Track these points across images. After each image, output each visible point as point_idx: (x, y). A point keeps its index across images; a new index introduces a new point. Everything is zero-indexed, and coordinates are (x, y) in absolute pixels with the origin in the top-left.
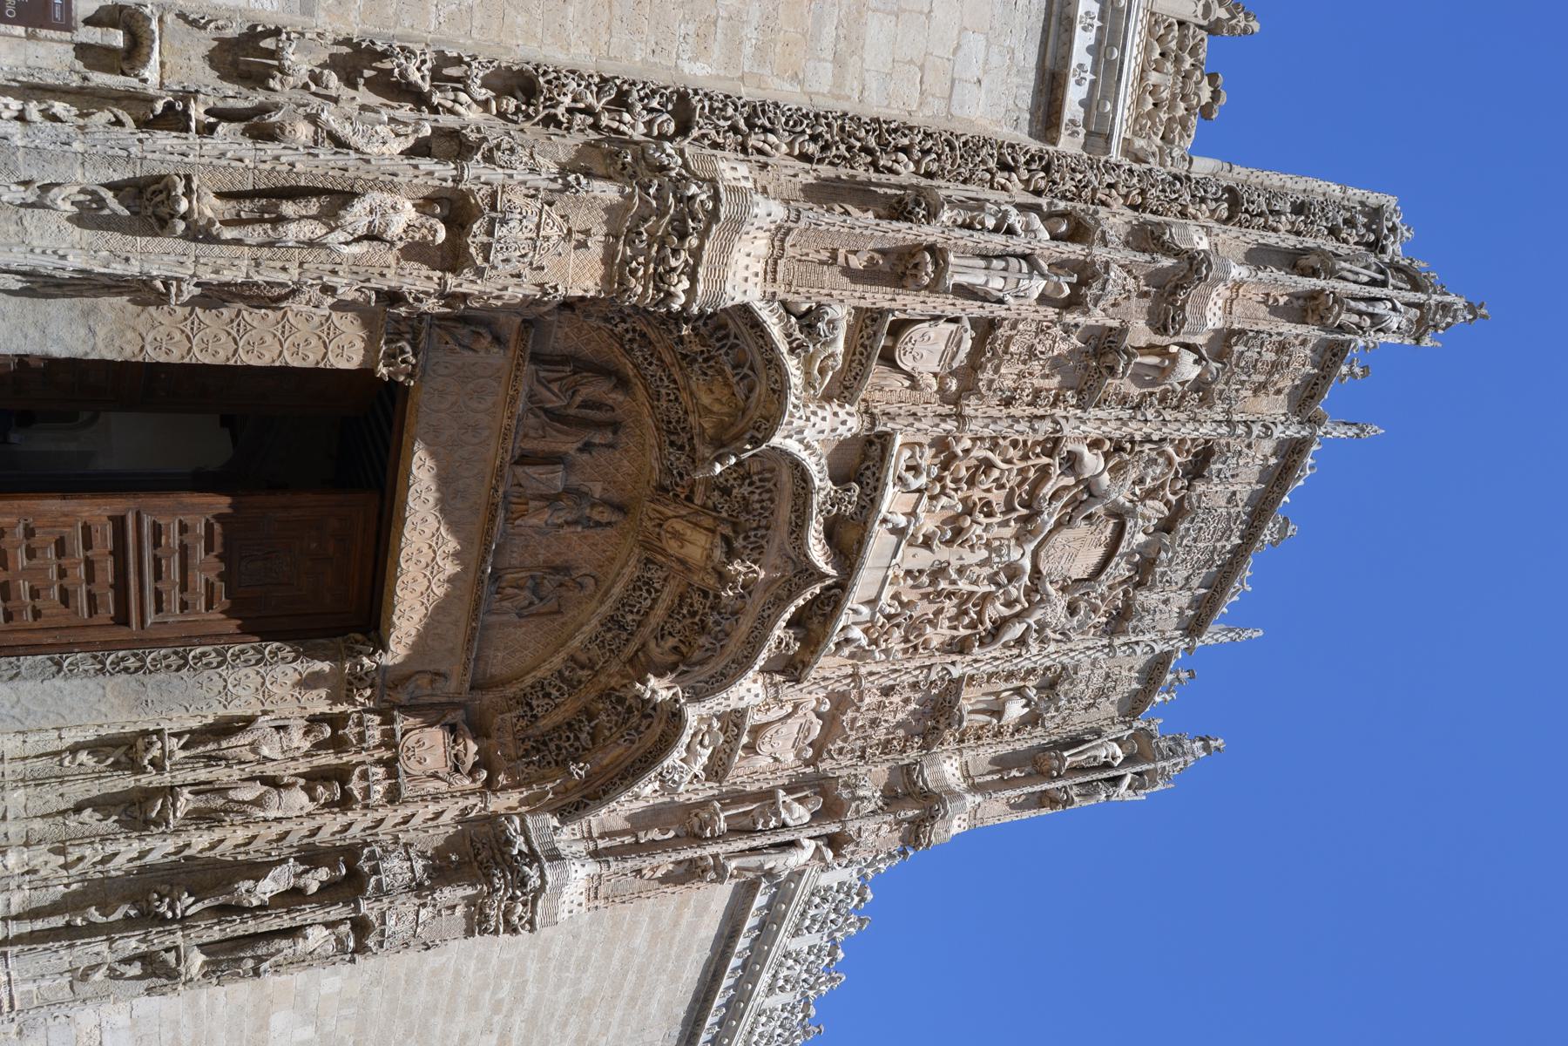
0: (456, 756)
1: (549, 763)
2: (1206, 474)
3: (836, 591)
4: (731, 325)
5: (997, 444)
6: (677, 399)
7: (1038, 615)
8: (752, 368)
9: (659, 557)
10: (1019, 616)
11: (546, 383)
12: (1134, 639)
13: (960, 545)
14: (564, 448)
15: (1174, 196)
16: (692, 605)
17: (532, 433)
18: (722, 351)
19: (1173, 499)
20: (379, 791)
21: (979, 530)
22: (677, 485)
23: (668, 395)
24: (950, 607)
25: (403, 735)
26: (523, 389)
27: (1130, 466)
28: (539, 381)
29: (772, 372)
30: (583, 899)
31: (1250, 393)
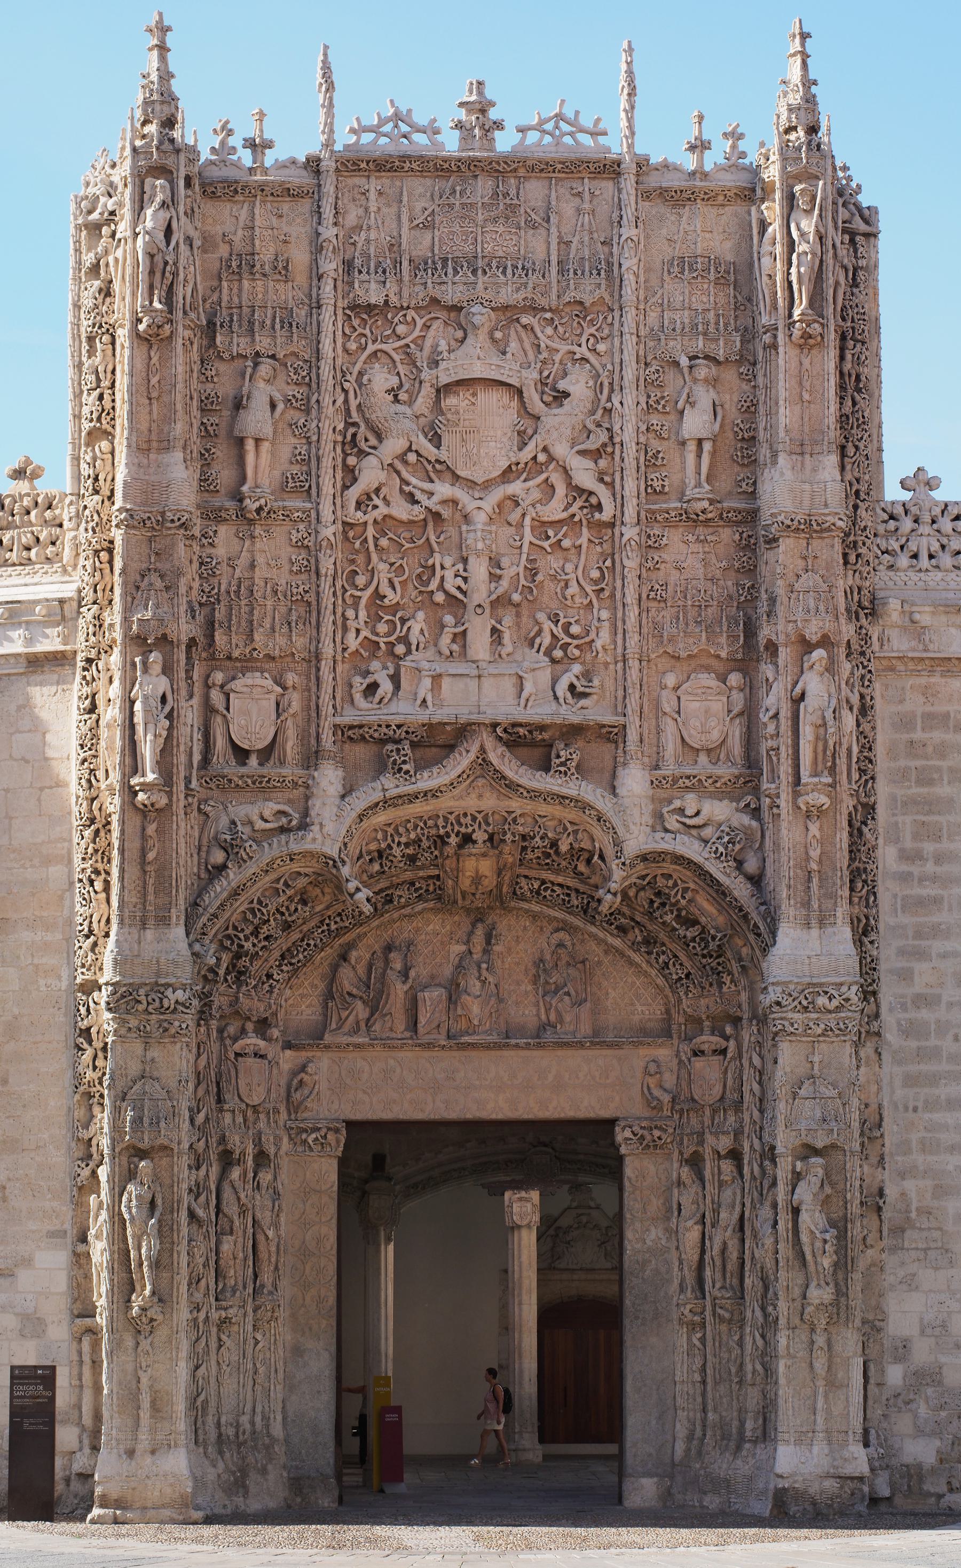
3: (499, 730)
4: (242, 909)
6: (339, 914)
7: (561, 450)
9: (505, 889)
10: (565, 471)
11: (342, 1022)
13: (464, 593)
14: (401, 995)
15: (96, 517)
16: (539, 858)
17: (389, 1025)
18: (264, 911)
21: (449, 574)
22: (427, 890)
23: (336, 923)
25: (693, 1100)
26: (346, 1039)
27: (373, 417)
28: (339, 1028)
29: (275, 866)
30: (830, 930)
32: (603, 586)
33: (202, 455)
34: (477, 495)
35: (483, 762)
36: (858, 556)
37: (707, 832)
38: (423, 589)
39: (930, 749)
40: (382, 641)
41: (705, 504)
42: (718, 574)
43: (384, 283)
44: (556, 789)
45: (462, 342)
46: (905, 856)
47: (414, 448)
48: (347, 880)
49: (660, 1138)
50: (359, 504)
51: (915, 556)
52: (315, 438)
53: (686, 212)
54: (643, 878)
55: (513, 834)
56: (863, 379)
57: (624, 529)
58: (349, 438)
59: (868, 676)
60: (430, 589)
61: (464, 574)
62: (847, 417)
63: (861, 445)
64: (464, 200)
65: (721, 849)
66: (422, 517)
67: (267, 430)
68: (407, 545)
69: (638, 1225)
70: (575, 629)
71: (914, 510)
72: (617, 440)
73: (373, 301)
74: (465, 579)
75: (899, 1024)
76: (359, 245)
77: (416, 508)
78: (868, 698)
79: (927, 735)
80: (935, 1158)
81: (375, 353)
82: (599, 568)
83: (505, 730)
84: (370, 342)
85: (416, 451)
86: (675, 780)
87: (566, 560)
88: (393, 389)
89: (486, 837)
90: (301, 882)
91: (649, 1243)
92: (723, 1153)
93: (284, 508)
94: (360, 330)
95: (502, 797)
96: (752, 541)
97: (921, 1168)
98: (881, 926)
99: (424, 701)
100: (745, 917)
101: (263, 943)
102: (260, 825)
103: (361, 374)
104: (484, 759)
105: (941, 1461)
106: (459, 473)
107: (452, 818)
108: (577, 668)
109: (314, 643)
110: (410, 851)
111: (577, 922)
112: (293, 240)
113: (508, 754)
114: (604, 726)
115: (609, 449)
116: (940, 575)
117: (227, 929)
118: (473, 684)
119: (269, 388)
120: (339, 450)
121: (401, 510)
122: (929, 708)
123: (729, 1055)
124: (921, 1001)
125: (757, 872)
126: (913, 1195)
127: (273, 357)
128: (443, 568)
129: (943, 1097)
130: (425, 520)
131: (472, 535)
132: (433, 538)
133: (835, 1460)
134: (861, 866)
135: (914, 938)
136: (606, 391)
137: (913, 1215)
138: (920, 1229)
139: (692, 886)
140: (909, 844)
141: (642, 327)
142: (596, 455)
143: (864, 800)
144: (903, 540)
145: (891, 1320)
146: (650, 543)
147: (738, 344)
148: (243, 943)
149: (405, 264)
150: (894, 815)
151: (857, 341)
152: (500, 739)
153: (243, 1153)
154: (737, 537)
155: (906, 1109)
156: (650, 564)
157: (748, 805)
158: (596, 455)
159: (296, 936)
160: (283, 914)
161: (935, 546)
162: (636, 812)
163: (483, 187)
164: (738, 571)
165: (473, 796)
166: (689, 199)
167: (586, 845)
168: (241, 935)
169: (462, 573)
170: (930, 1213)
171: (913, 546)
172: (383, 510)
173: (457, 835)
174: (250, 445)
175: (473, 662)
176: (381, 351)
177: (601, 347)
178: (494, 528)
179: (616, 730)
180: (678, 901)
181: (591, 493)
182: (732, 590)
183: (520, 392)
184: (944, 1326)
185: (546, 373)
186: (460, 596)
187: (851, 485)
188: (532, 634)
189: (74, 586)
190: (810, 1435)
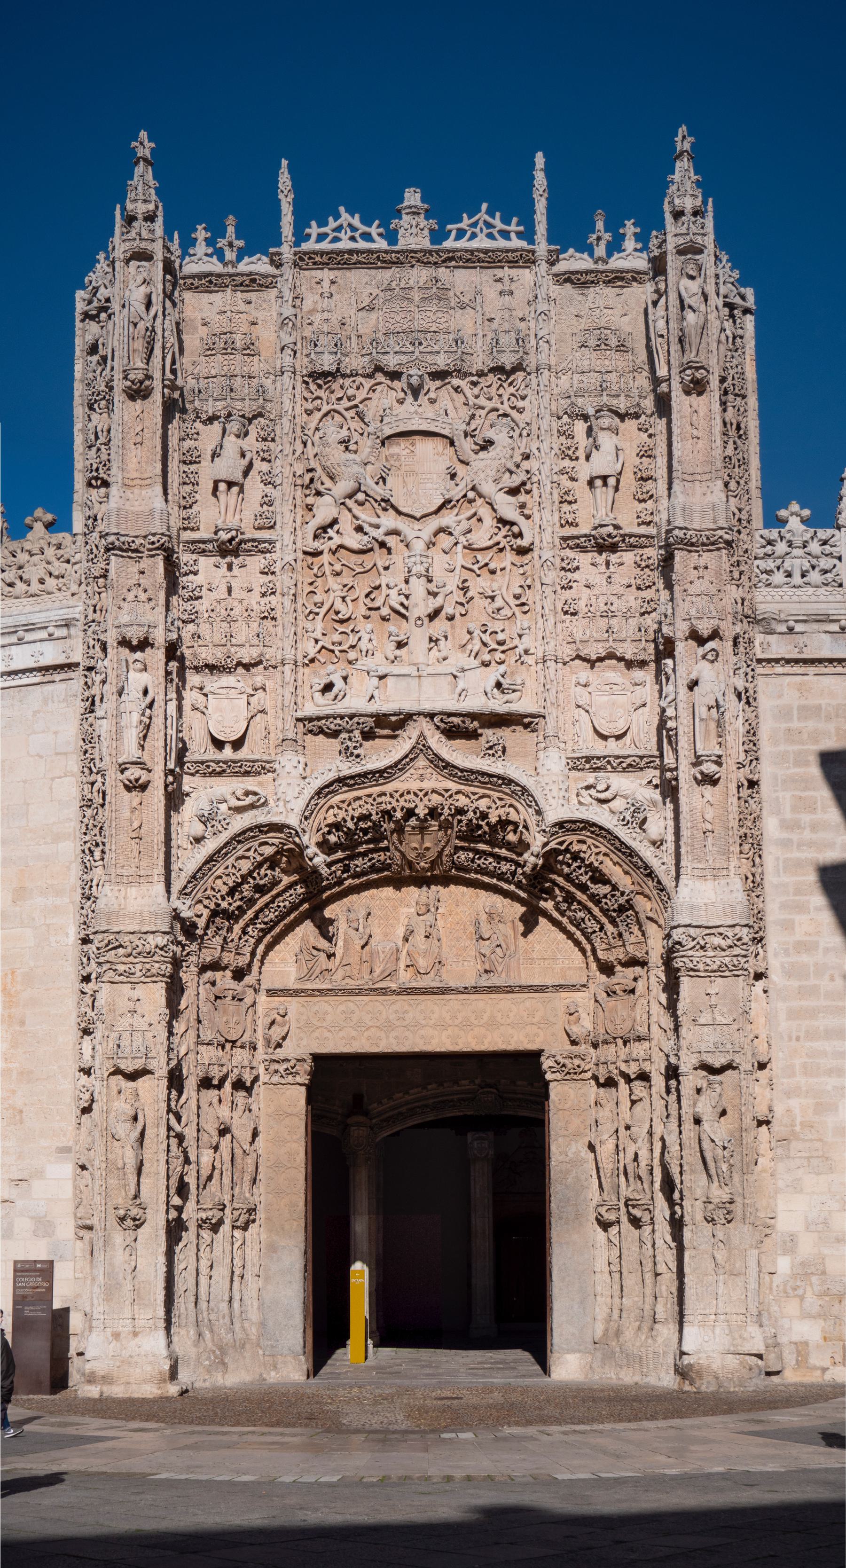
0: (625, 991)
1: (628, 917)
2: (334, 368)
3: (436, 719)
4: (218, 873)
5: (311, 612)
7: (487, 488)
8: (249, 850)
9: (445, 859)
12: (533, 342)
13: (406, 608)
15: (95, 550)
19: (368, 383)
20: (638, 1049)
24: (480, 584)
27: (328, 464)
31: (256, 358)
32: (523, 600)
33: (184, 498)
34: (417, 525)
35: (421, 748)
36: (741, 573)
37: (618, 804)
38: (370, 605)
39: (805, 736)
40: (336, 649)
41: (611, 529)
42: (622, 590)
43: (336, 353)
44: (485, 768)
45: (402, 403)
46: (785, 825)
47: (363, 488)
48: (307, 847)
49: (579, 1066)
50: (316, 537)
51: (789, 575)
52: (278, 482)
53: (591, 291)
54: (561, 843)
55: (450, 809)
56: (743, 426)
57: (543, 553)
58: (307, 481)
59: (751, 673)
60: (377, 604)
61: (407, 593)
62: (730, 459)
63: (742, 482)
64: (402, 285)
65: (628, 818)
66: (370, 546)
67: (238, 476)
68: (358, 570)
69: (560, 1140)
70: (501, 637)
71: (788, 536)
72: (535, 479)
73: (326, 368)
74: (407, 597)
75: (783, 967)
76: (315, 325)
77: (366, 538)
78: (751, 692)
79: (803, 724)
80: (816, 1080)
81: (329, 412)
82: (521, 586)
83: (442, 720)
84: (325, 403)
85: (365, 492)
86: (588, 759)
87: (493, 580)
88: (344, 441)
89: (427, 811)
90: (268, 851)
91: (570, 1155)
92: (633, 1077)
93: (254, 540)
94: (317, 394)
95: (441, 778)
96: (651, 561)
97: (804, 1089)
98: (766, 884)
99: (372, 697)
100: (650, 874)
101: (238, 903)
102: (234, 803)
103: (317, 429)
104: (424, 745)
105: (825, 1339)
106: (401, 509)
107: (397, 795)
108: (502, 668)
109: (280, 651)
110: (362, 825)
111: (505, 886)
112: (260, 322)
113: (443, 739)
114: (526, 716)
115: (528, 487)
116: (811, 590)
117: (206, 890)
118: (414, 682)
119: (240, 441)
120: (299, 493)
121: (354, 541)
122: (803, 702)
123: (637, 993)
124: (803, 947)
125: (660, 838)
126: (797, 1111)
127: (243, 416)
128: (387, 586)
129: (821, 1028)
130: (371, 550)
131: (413, 559)
132: (380, 564)
133: (734, 1339)
134: (748, 831)
135: (795, 894)
136: (525, 440)
137: (798, 1128)
138: (804, 1140)
139: (603, 849)
140: (788, 815)
141: (554, 386)
142: (513, 492)
143: (751, 777)
144: (779, 562)
145: (780, 1217)
146: (564, 565)
147: (637, 399)
148: (220, 902)
149: (354, 338)
150: (776, 791)
151: (736, 395)
152: (438, 728)
153: (222, 1080)
154: (638, 558)
155: (790, 1038)
156: (564, 582)
157: (650, 782)
158: (513, 492)
159: (267, 898)
160: (254, 879)
161: (806, 566)
162: (555, 788)
163: (419, 275)
164: (639, 588)
165: (415, 777)
166: (593, 282)
167: (513, 816)
168: (218, 895)
169: (404, 591)
170: (812, 1127)
171: (787, 565)
172: (337, 540)
173: (402, 809)
174: (222, 486)
175: (414, 664)
176: (335, 411)
177: (520, 404)
178: (430, 553)
179: (536, 720)
180: (592, 863)
181: (512, 524)
182: (633, 603)
183: (452, 444)
184: (825, 1223)
185: (473, 427)
186: (403, 611)
187: (734, 514)
188: (464, 642)
189: (78, 610)
190: (713, 1317)
